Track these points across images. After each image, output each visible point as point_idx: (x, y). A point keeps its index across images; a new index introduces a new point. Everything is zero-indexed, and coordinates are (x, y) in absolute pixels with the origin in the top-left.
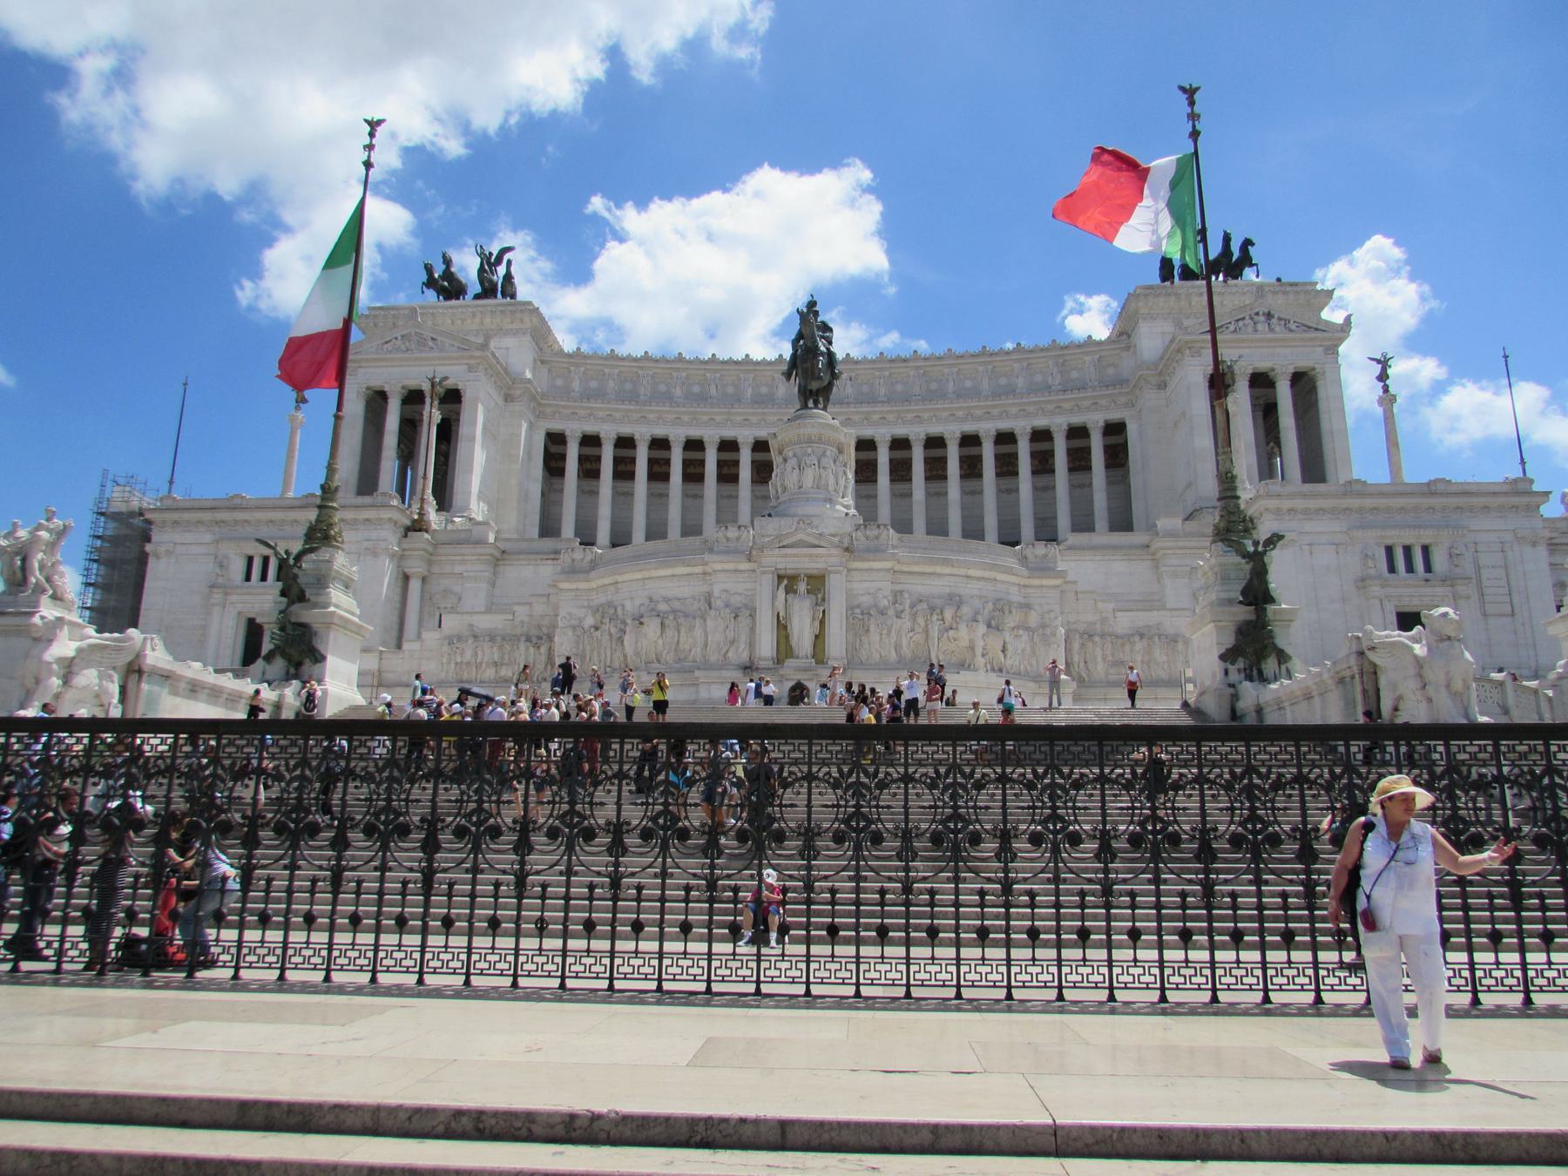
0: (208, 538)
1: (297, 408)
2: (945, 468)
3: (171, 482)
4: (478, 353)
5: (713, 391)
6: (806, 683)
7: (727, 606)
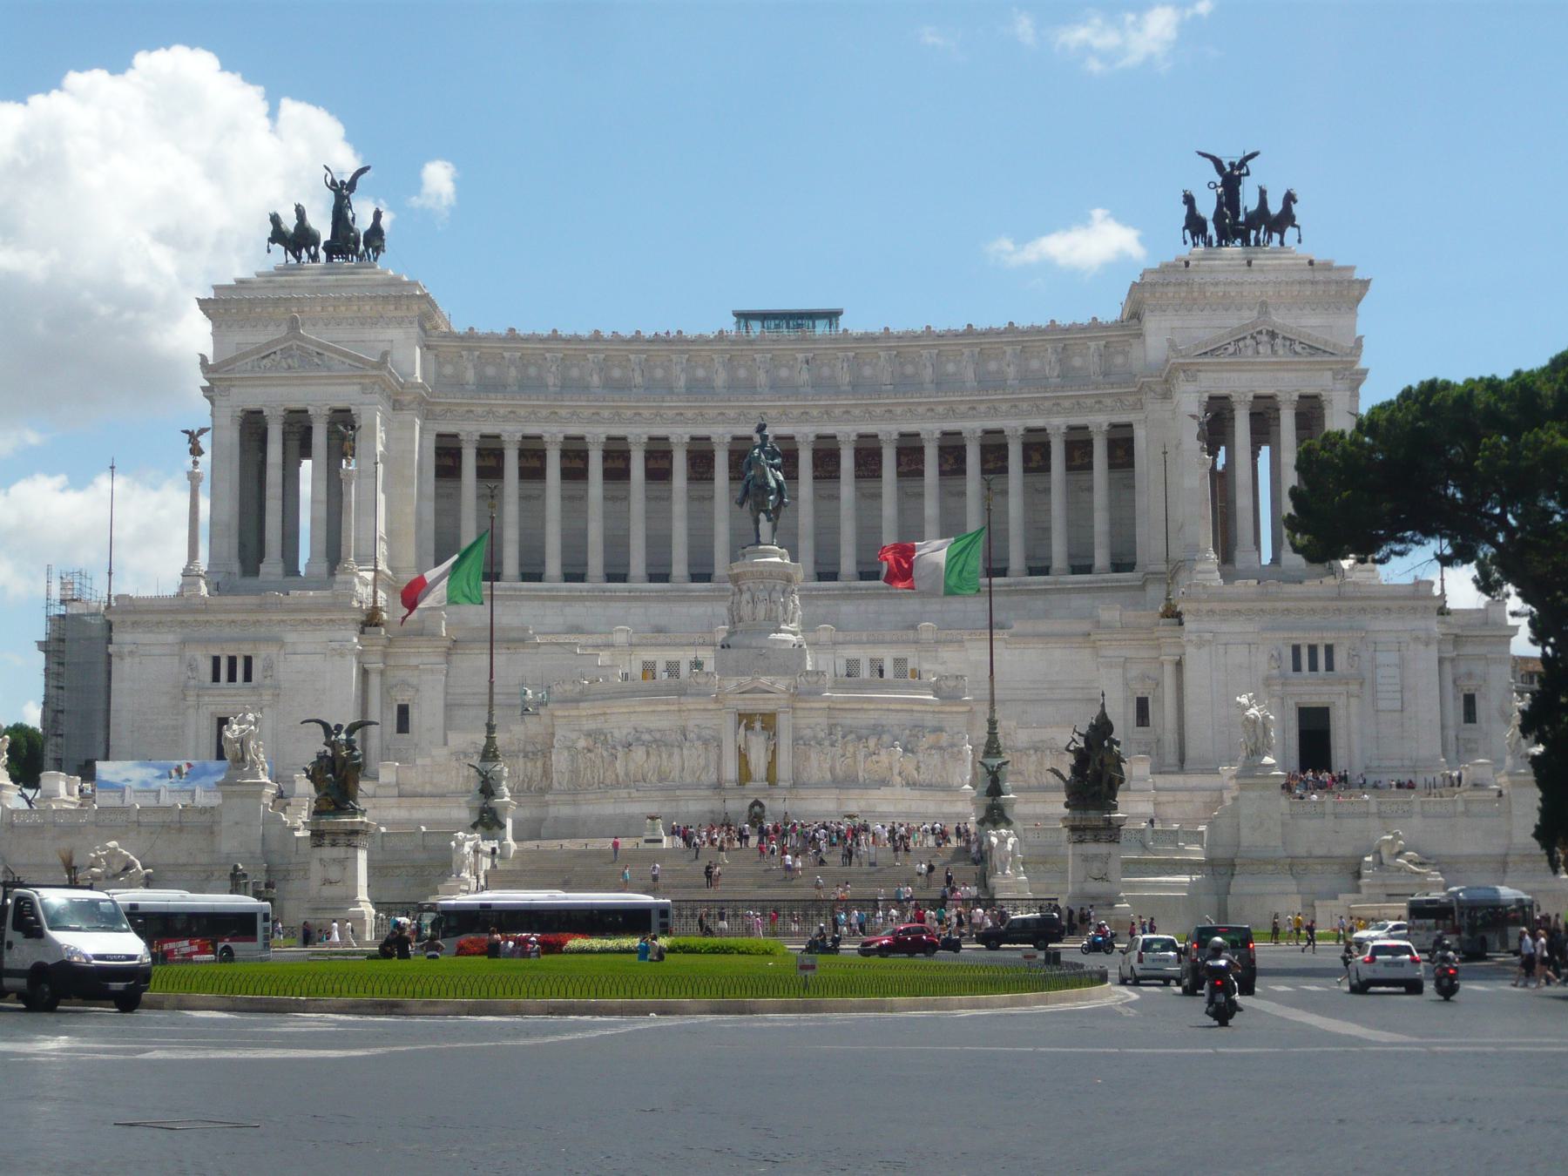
0: (170, 638)
1: (195, 463)
2: (922, 462)
3: (110, 574)
4: (375, 373)
5: (638, 379)
6: (764, 802)
7: (699, 738)
